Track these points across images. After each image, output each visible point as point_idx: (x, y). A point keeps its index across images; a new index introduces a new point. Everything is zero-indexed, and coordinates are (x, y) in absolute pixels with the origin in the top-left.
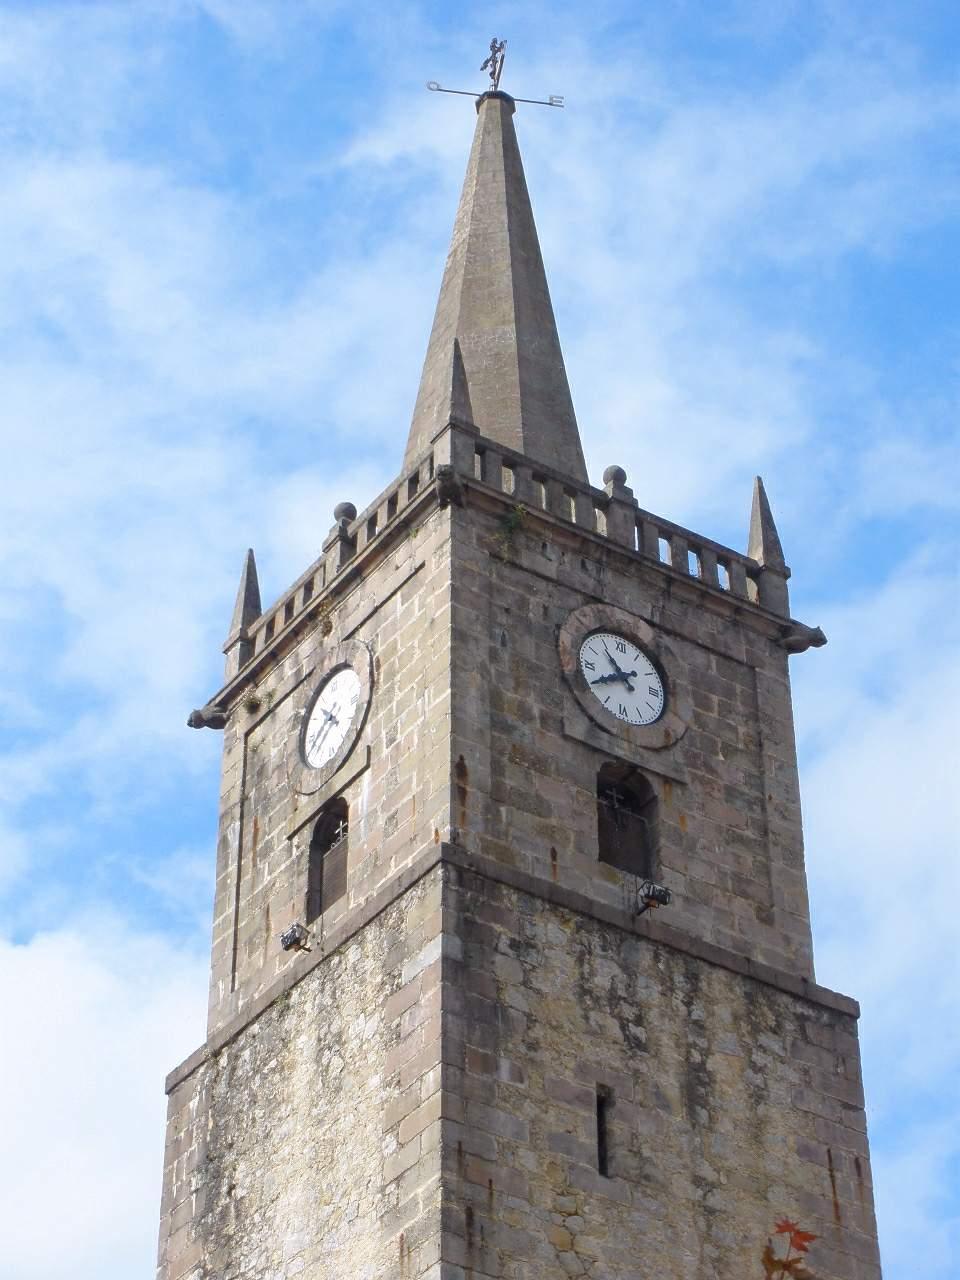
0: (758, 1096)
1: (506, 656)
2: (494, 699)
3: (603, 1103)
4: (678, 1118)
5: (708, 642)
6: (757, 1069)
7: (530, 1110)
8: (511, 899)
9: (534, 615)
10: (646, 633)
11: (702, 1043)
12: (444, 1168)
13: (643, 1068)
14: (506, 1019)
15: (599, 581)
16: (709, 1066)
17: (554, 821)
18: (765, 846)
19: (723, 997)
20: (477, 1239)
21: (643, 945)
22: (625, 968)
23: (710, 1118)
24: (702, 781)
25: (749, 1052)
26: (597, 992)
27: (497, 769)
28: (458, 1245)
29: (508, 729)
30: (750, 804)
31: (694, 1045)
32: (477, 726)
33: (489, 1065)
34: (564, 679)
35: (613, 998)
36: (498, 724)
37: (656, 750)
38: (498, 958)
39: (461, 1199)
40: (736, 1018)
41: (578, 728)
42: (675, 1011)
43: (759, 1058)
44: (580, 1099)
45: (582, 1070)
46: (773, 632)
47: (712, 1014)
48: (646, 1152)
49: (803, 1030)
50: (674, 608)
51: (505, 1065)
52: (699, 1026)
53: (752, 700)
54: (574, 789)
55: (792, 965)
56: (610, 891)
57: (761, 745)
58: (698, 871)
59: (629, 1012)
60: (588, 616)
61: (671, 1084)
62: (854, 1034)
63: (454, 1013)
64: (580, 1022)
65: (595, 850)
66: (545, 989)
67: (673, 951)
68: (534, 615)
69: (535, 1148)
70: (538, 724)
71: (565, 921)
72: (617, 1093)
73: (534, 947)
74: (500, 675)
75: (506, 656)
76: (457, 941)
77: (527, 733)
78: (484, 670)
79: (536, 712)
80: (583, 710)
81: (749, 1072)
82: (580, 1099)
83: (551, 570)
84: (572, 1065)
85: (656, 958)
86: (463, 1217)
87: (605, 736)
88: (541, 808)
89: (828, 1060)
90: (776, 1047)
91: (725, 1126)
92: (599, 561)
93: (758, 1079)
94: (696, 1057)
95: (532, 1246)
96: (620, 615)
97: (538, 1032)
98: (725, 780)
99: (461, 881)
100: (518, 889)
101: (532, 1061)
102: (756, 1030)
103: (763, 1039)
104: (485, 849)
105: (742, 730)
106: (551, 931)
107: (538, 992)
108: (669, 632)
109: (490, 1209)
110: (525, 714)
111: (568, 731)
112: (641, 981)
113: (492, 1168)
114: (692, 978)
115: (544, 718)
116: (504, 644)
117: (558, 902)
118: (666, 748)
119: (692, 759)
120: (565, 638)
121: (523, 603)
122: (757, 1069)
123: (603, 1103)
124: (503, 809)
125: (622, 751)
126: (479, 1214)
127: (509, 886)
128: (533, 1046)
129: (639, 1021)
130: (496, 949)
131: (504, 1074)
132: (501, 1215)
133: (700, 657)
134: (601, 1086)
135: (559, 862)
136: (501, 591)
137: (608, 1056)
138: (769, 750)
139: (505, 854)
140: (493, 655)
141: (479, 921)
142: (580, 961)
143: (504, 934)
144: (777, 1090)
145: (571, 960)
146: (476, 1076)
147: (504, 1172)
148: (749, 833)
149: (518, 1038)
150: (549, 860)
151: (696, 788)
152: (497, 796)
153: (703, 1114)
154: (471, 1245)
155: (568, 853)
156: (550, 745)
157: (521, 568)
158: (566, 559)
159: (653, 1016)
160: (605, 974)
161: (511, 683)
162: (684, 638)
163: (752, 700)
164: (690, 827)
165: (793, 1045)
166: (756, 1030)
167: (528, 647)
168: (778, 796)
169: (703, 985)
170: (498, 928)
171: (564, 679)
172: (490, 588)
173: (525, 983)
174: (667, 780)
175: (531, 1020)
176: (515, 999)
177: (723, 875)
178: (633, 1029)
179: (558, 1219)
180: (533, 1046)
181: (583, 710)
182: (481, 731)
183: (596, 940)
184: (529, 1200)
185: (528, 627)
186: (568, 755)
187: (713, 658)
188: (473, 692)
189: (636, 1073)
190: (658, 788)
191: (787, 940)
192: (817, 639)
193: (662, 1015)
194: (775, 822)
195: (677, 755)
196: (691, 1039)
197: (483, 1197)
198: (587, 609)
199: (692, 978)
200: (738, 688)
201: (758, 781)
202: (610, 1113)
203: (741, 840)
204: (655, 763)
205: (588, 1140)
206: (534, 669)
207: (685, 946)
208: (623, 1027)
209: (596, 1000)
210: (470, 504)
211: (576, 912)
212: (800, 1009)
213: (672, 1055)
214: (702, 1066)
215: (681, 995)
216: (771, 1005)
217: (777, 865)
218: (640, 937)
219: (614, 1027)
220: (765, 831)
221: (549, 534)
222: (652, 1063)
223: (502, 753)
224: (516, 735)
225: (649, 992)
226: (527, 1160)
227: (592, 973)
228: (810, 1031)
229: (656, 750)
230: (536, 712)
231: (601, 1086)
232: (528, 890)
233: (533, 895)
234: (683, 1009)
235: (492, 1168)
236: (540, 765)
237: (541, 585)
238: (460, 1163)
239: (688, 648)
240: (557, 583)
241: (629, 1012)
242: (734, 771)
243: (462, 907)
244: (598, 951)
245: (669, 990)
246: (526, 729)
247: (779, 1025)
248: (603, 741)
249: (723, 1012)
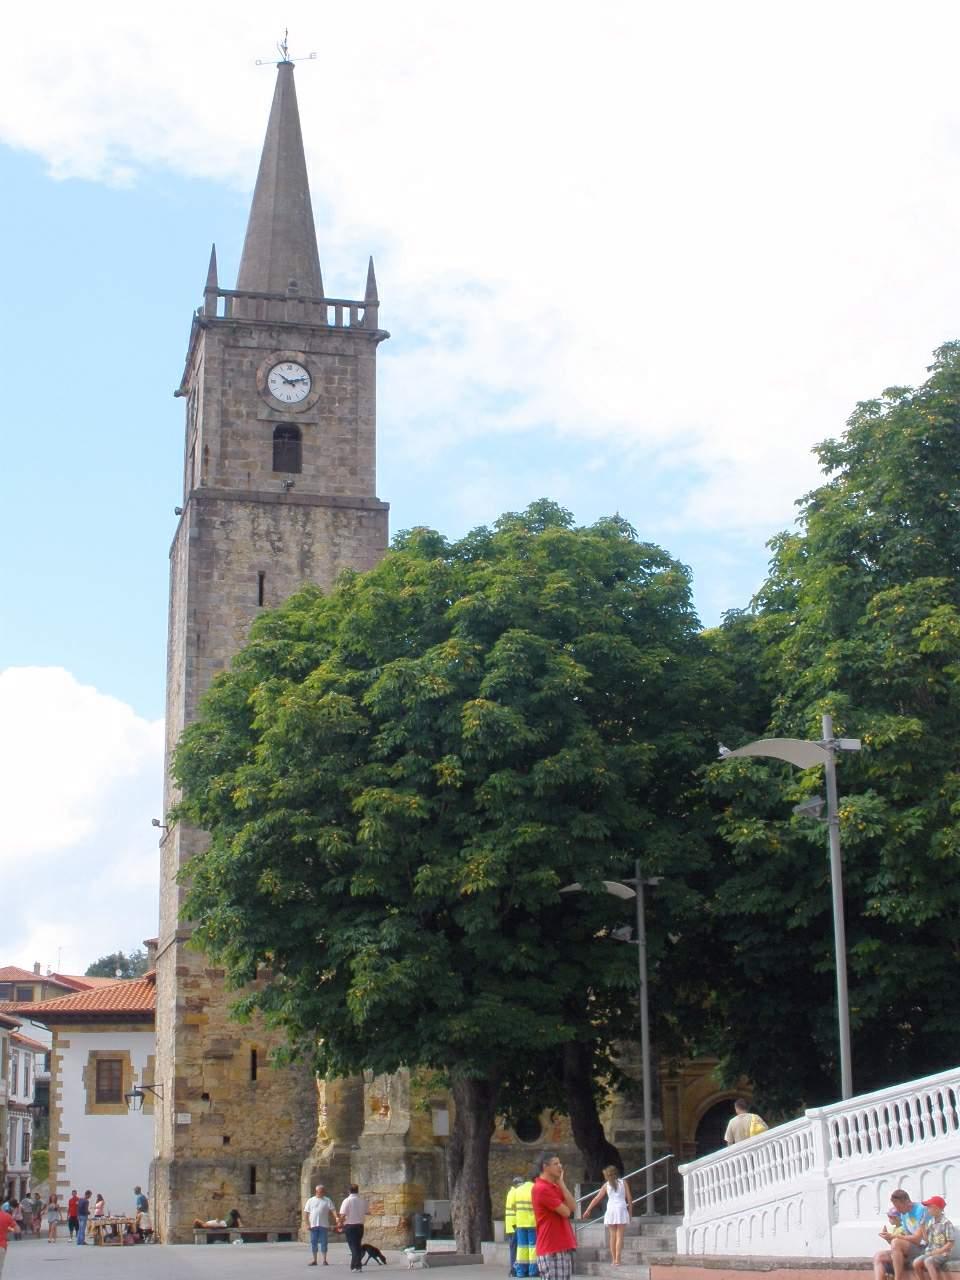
0: (335, 556)
1: (230, 392)
2: (224, 412)
3: (262, 577)
4: (296, 575)
5: (334, 352)
6: (335, 545)
7: (227, 589)
8: (221, 504)
9: (246, 367)
10: (301, 358)
11: (309, 541)
12: (188, 621)
13: (280, 559)
14: (218, 555)
15: (279, 341)
16: (312, 550)
17: (251, 459)
18: (356, 440)
19: (321, 517)
20: (202, 645)
21: (283, 507)
22: (274, 520)
23: (311, 572)
24: (326, 419)
25: (332, 539)
26: (260, 533)
27: (224, 444)
28: (193, 650)
29: (230, 425)
30: (350, 423)
31: (305, 543)
32: (215, 428)
33: (208, 576)
34: (259, 393)
35: (268, 533)
36: (225, 423)
37: (303, 412)
38: (215, 531)
39: (194, 631)
40: (327, 527)
41: (264, 414)
42: (298, 531)
43: (337, 540)
44: (250, 579)
45: (251, 568)
46: (368, 336)
47: (316, 527)
48: (280, 593)
49: (360, 523)
50: (317, 341)
51: (216, 574)
52: (309, 535)
53: (355, 372)
54: (261, 442)
55: (364, 491)
56: (272, 485)
57: (357, 393)
58: (321, 462)
59: (275, 537)
60: (272, 359)
61: (293, 562)
62: (386, 518)
63: (194, 559)
64: (252, 548)
65: (271, 466)
66: (236, 538)
67: (297, 505)
68: (246, 367)
69: (229, 604)
70: (245, 418)
71: (246, 507)
72: (267, 571)
73: (232, 522)
74: (228, 401)
75: (230, 392)
76: (196, 529)
77: (239, 424)
78: (220, 402)
79: (244, 412)
80: (268, 405)
81: (332, 548)
82: (250, 579)
83: (254, 343)
84: (247, 566)
85: (290, 510)
86: (196, 638)
87: (277, 413)
88: (246, 455)
89: (372, 531)
90: (346, 534)
91: (318, 573)
92: (279, 331)
93: (336, 549)
94: (306, 547)
95: (225, 642)
96: (288, 354)
97: (233, 557)
98: (339, 415)
99: (198, 504)
100: (225, 500)
101: (229, 570)
102: (336, 528)
103: (340, 532)
104: (216, 483)
105: (349, 388)
106: (241, 513)
107: (233, 540)
108: (314, 353)
109: (207, 632)
110: (239, 415)
111: (259, 417)
112: (282, 522)
113: (208, 617)
114: (307, 515)
115: (248, 414)
116: (230, 386)
117: (243, 499)
118: (309, 409)
119: (321, 411)
120: (260, 374)
121: (240, 363)
122: (335, 545)
123: (262, 577)
124: (227, 462)
125: (286, 418)
126: (203, 636)
127: (221, 500)
128: (229, 564)
129: (280, 540)
130: (214, 528)
131: (215, 579)
132: (212, 634)
133: (330, 359)
134: (260, 572)
135: (252, 478)
136: (229, 361)
137: (264, 558)
138: (362, 393)
139: (225, 483)
140: (224, 393)
141: (206, 518)
142: (253, 521)
143: (217, 520)
144: (345, 551)
145: (249, 523)
146: (203, 582)
147: (214, 616)
148: (349, 436)
149: (222, 562)
150: (246, 479)
151: (322, 423)
152: (223, 456)
153: (307, 571)
154: (198, 648)
155: (256, 472)
156: (253, 426)
157: (239, 347)
158: (263, 336)
159: (287, 536)
160: (265, 523)
161: (233, 403)
162: (321, 354)
163: (355, 372)
164: (319, 442)
165: (355, 530)
166: (336, 528)
167: (242, 384)
168: (364, 415)
169: (312, 516)
170: (215, 518)
171: (259, 393)
172: (224, 362)
173: (227, 538)
174: (308, 425)
175: (229, 552)
176: (222, 546)
177: (334, 460)
178: (277, 544)
179: (237, 629)
180: (229, 564)
181: (268, 405)
182: (217, 431)
183: (261, 510)
184: (225, 625)
185: (242, 374)
186: (259, 427)
187: (337, 359)
188: (213, 414)
189: (277, 562)
190: (303, 429)
191: (362, 480)
192: (386, 335)
193: (291, 533)
194: (362, 427)
195: (314, 411)
196: (304, 540)
197: (205, 628)
198: (272, 357)
199: (307, 515)
200: (349, 368)
201: (353, 411)
202: (265, 581)
203: (345, 441)
204: (302, 419)
205: (253, 594)
206: (244, 393)
207: (304, 502)
208: (272, 544)
209: (259, 536)
210: (215, 326)
211: (251, 501)
212: (360, 514)
213: (294, 549)
214: (309, 551)
215: (300, 523)
216: (345, 514)
217: (361, 447)
218: (282, 504)
219: (268, 546)
220: (355, 432)
221: (253, 327)
222: (285, 555)
223: (227, 436)
224: (235, 427)
225: (286, 526)
226: (225, 609)
227: (259, 525)
228: (364, 521)
229: (303, 412)
230: (244, 412)
231: (260, 572)
232: (229, 499)
233: (232, 501)
234: (301, 529)
235: (208, 617)
236: (246, 437)
237: (250, 352)
238: (195, 618)
239: (324, 358)
240: (257, 348)
241: (275, 537)
242: (342, 410)
243: (199, 514)
244: (262, 515)
245: (294, 521)
246: (239, 422)
247: (349, 523)
248: (277, 417)
249: (321, 525)
